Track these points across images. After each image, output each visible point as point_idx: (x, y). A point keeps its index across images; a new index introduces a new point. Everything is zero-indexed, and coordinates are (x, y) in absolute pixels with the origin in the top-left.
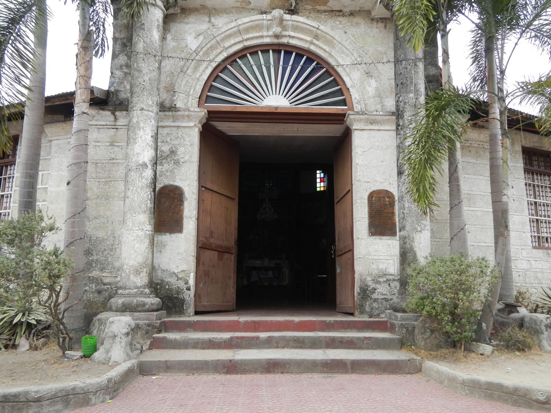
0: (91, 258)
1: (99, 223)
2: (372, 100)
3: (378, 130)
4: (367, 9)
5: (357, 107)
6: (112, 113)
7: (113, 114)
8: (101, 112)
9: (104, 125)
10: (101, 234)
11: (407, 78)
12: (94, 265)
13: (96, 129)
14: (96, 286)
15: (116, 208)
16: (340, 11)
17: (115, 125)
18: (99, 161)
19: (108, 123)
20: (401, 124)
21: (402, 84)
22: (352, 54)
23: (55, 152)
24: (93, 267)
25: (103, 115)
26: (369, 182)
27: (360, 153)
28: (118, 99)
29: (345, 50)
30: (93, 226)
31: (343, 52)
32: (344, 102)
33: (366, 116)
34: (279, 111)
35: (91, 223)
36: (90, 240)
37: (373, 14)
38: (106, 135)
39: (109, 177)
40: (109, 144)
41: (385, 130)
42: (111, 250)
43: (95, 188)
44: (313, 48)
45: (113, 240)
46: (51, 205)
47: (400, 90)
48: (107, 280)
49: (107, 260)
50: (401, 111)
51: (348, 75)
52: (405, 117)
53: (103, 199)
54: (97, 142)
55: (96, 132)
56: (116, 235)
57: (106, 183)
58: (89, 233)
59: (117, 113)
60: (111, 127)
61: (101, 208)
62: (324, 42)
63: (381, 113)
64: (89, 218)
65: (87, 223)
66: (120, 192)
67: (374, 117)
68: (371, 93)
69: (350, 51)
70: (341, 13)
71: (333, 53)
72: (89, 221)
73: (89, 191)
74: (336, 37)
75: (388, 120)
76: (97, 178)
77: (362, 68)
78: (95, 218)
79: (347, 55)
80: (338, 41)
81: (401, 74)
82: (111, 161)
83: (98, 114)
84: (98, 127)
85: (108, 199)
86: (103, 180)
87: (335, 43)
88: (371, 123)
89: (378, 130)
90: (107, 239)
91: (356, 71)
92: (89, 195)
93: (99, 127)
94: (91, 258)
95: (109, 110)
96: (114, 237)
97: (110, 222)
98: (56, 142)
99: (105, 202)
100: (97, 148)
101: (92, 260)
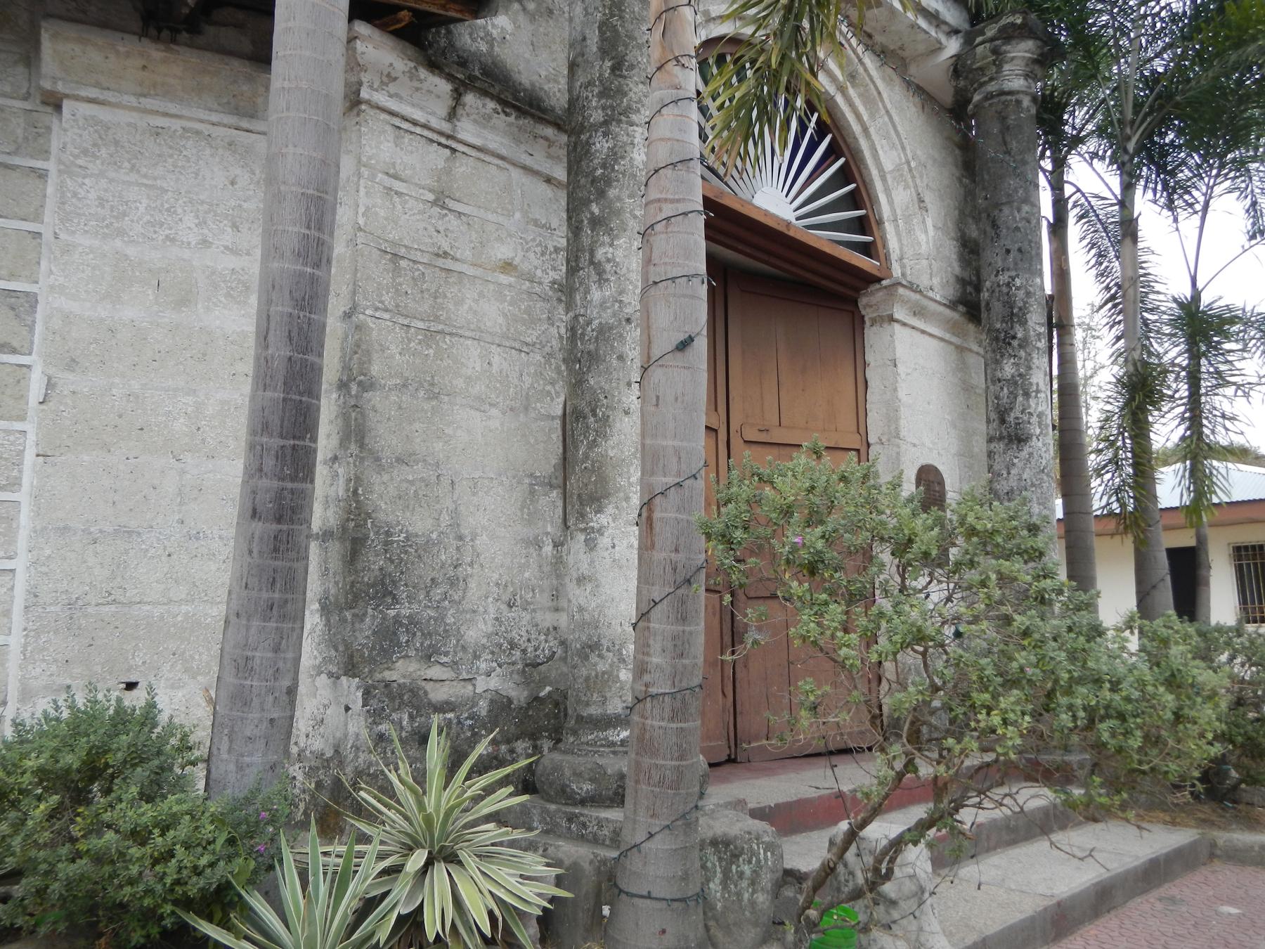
0: (392, 613)
1: (412, 483)
2: (925, 262)
3: (923, 332)
4: (905, 54)
5: (896, 271)
6: (456, 90)
7: (458, 95)
8: (423, 73)
9: (415, 123)
10: (419, 523)
11: (1030, 241)
12: (404, 639)
13: (388, 128)
14: (411, 717)
15: (459, 433)
16: (870, 36)
17: (449, 137)
18: (402, 251)
19: (435, 123)
20: (1019, 335)
21: (1020, 250)
22: (903, 148)
23: (85, 152)
24: (399, 645)
25: (425, 86)
26: (915, 445)
27: (903, 376)
28: (452, 45)
29: (892, 132)
30: (392, 491)
31: (887, 137)
32: (867, 249)
33: (918, 296)
34: (791, 233)
35: (386, 477)
36: (386, 543)
37: (913, 69)
38: (421, 160)
39: (437, 319)
40: (431, 197)
41: (931, 335)
42: (453, 582)
43: (393, 347)
44: (839, 99)
45: (458, 549)
46: (71, 376)
47: (1016, 264)
48: (438, 694)
49: (441, 619)
50: (1020, 309)
51: (887, 191)
52: (1030, 323)
53: (421, 393)
54: (396, 177)
55: (391, 138)
56: (465, 532)
57: (430, 336)
58: (382, 516)
59: (470, 98)
60: (435, 137)
61: (417, 426)
62: (860, 95)
63: (938, 298)
64: (378, 459)
65: (375, 479)
66: (469, 379)
67: (925, 302)
68: (924, 247)
69: (900, 139)
70: (870, 42)
71: (872, 130)
72: (381, 469)
73: (375, 356)
74: (885, 95)
75: (940, 313)
76: (398, 311)
77: (916, 186)
78: (398, 460)
79: (893, 147)
80: (885, 107)
81: (1017, 229)
82: (440, 262)
83: (412, 76)
84: (397, 122)
85: (436, 396)
86: (421, 325)
87: (878, 109)
88: (915, 314)
89: (923, 332)
90: (440, 543)
91: (901, 188)
92: (375, 369)
93: (403, 124)
94: (392, 613)
95: (450, 77)
96: (461, 538)
97: (445, 482)
98: (85, 109)
99: (427, 406)
100: (396, 199)
101: (397, 620)
